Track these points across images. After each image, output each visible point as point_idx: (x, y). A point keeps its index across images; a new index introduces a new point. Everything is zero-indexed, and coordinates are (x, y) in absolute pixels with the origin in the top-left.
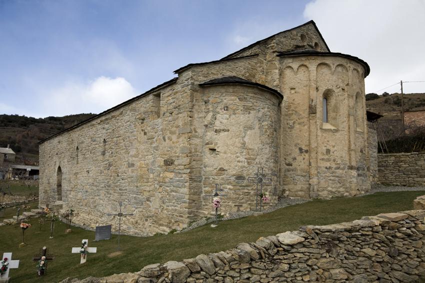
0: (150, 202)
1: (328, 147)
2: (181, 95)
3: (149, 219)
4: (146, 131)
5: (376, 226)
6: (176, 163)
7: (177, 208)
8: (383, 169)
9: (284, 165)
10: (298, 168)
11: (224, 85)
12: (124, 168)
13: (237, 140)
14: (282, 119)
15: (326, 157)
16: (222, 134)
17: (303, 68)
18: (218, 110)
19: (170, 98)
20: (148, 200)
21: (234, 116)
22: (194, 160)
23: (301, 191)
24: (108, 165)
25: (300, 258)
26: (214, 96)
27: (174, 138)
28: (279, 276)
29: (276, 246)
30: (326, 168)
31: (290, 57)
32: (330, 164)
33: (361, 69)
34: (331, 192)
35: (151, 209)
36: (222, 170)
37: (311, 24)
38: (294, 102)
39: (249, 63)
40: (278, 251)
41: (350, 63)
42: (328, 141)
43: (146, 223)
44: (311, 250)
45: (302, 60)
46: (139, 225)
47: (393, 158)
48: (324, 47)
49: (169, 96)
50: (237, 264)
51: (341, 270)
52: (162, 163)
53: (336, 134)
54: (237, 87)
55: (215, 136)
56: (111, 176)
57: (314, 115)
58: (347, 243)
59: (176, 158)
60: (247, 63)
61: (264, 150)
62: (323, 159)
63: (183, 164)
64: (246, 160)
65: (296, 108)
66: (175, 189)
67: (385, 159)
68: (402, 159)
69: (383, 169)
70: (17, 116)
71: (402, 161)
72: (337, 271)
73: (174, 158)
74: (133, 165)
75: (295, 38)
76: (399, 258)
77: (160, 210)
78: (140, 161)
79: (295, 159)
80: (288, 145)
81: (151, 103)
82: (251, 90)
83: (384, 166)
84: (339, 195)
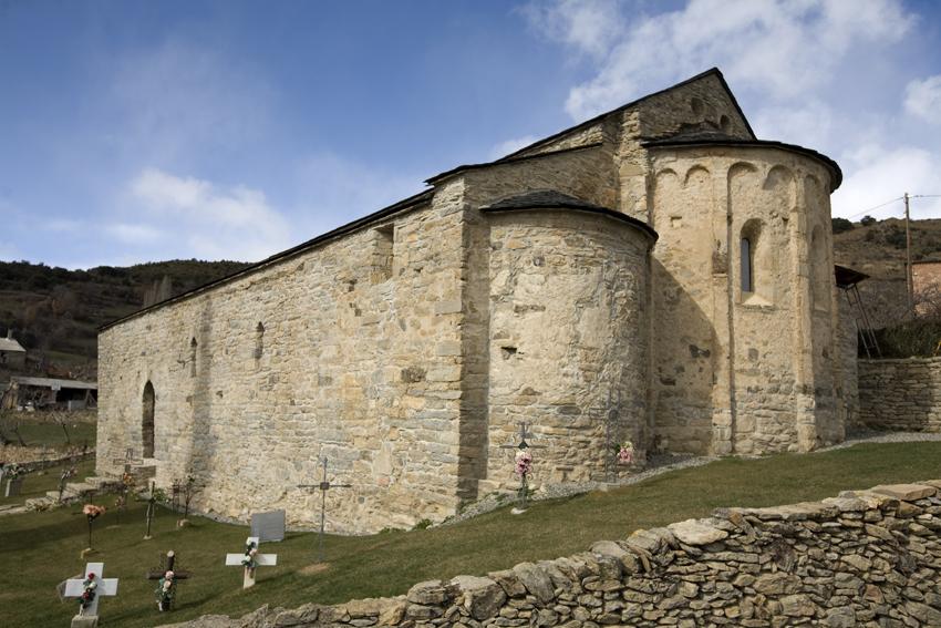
0: (370, 460)
1: (754, 345)
2: (442, 231)
3: (366, 498)
4: (360, 307)
5: (870, 509)
6: (429, 377)
7: (432, 474)
8: (870, 392)
9: (658, 382)
10: (689, 389)
11: (535, 212)
12: (307, 386)
13: (562, 328)
14: (653, 282)
15: (749, 366)
16: (530, 315)
17: (698, 173)
18: (521, 264)
19: (416, 237)
20: (365, 455)
21: (555, 278)
22: (470, 372)
23: (694, 439)
24: (267, 380)
25: (720, 571)
26: (513, 234)
27: (426, 322)
28: (678, 608)
29: (671, 547)
30: (749, 389)
31: (669, 150)
32: (758, 381)
33: (822, 176)
34: (761, 442)
35: (372, 475)
36: (530, 392)
37: (714, 76)
38: (678, 247)
39: (583, 163)
40: (676, 557)
41: (800, 163)
42: (753, 332)
43: (361, 506)
44: (742, 557)
45: (696, 157)
46: (344, 510)
47: (891, 369)
48: (741, 125)
49: (413, 232)
50: (595, 581)
51: (802, 597)
52: (398, 378)
53: (769, 316)
54: (563, 216)
55: (517, 321)
56: (276, 404)
57: (724, 275)
58: (813, 543)
59: (431, 367)
61: (619, 350)
62: (742, 371)
63: (447, 379)
64: (581, 373)
65: (684, 258)
66: (427, 432)
67: (874, 371)
68: (914, 371)
69: (870, 392)
71: (911, 376)
72: (793, 598)
73: (424, 367)
74: (329, 380)
75: (679, 106)
76: (917, 575)
77: (392, 478)
78: (345, 372)
79: (681, 369)
80: (667, 339)
81: (371, 246)
82: (592, 223)
83: (873, 387)
84: (778, 448)
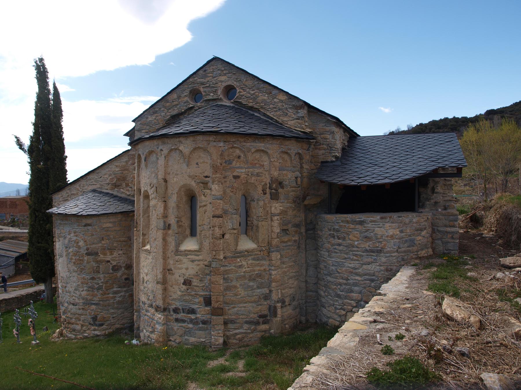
60: (114, 167)
61: (71, 278)
70: (446, 119)
75: (175, 103)
